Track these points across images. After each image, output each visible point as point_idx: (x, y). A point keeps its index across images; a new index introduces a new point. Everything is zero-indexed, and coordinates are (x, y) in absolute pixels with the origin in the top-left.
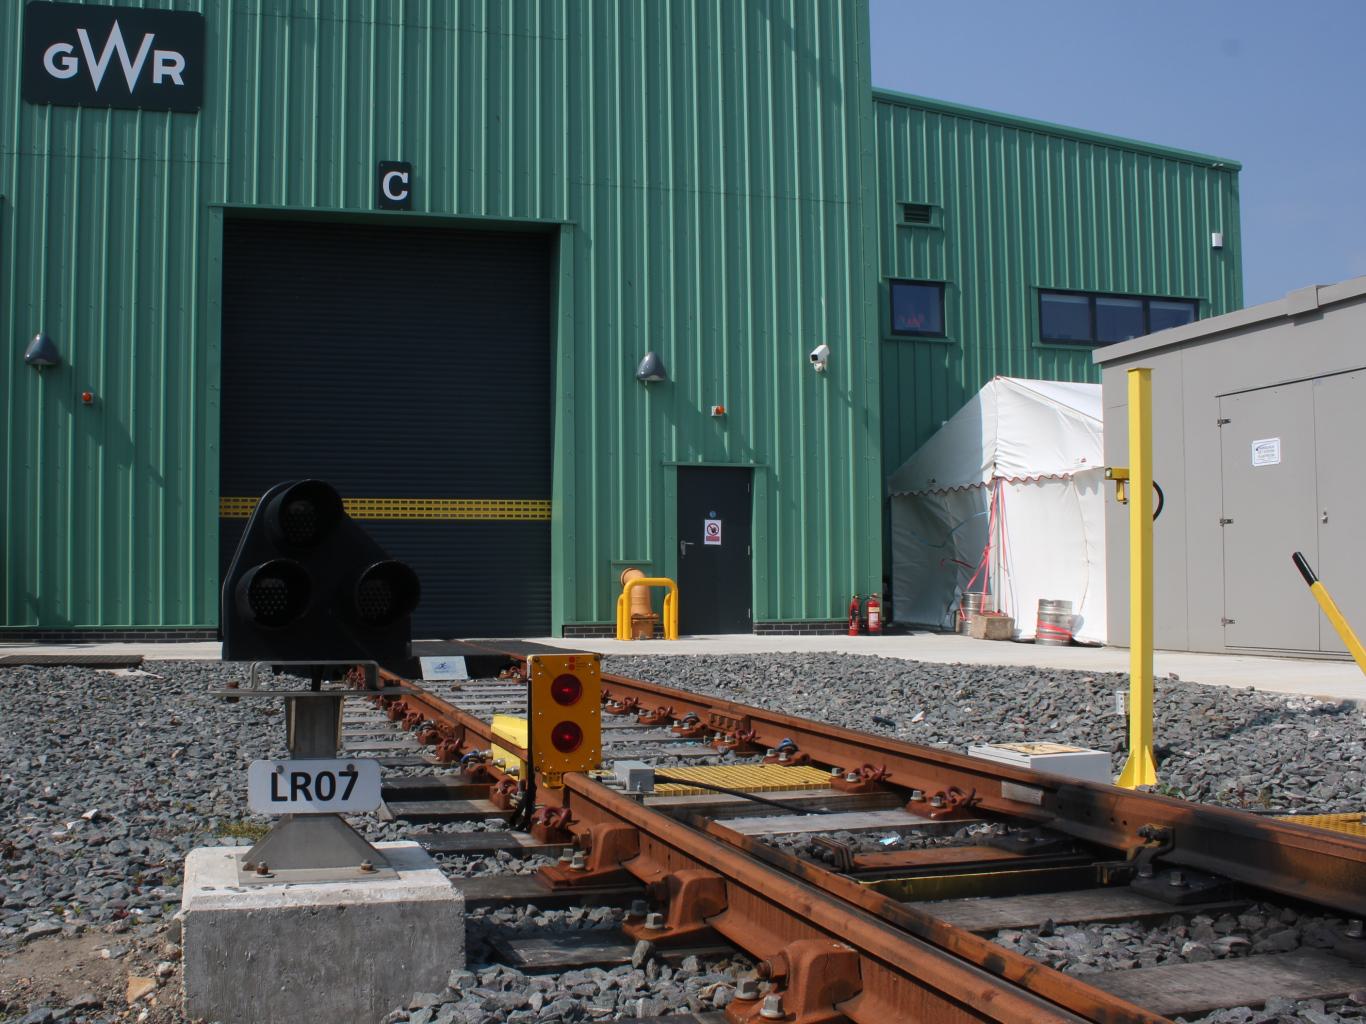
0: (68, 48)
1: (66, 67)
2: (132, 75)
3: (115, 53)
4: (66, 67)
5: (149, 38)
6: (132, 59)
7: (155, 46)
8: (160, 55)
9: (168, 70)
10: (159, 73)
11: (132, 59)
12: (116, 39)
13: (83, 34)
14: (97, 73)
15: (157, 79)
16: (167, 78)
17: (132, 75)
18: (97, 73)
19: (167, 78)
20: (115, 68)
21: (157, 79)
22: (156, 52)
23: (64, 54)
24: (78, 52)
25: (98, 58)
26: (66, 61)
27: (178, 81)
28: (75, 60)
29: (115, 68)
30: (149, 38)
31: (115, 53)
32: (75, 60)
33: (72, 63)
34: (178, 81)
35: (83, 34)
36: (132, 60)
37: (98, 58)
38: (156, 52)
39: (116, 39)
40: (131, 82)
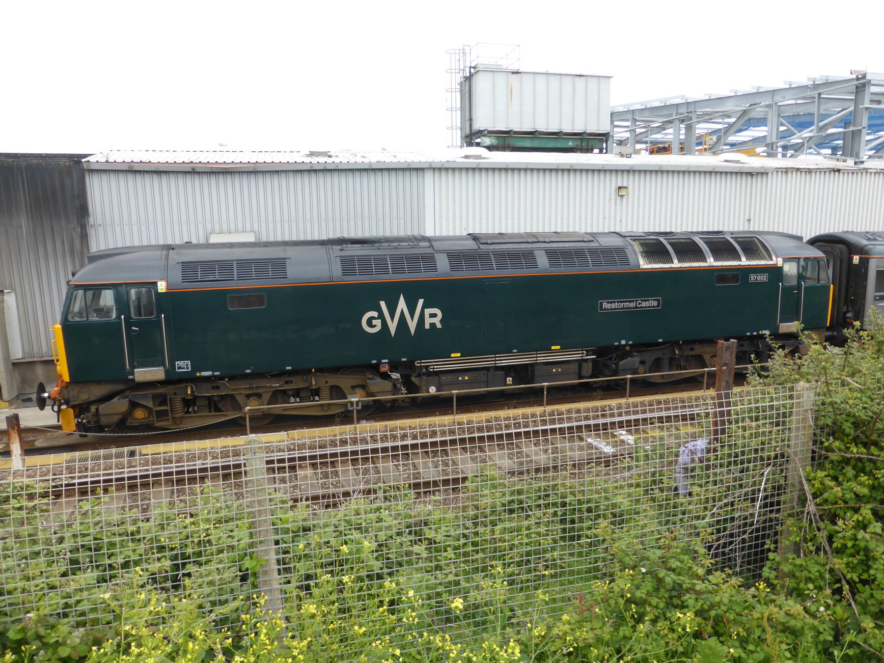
0: (375, 314)
1: (375, 326)
2: (412, 325)
4: (375, 326)
5: (421, 302)
6: (412, 316)
7: (425, 306)
8: (428, 311)
9: (433, 320)
10: (428, 321)
11: (412, 316)
12: (402, 305)
13: (383, 304)
14: (393, 327)
15: (427, 326)
16: (433, 325)
17: (412, 325)
18: (393, 327)
19: (433, 325)
21: (427, 326)
23: (372, 318)
24: (381, 316)
26: (374, 322)
27: (439, 326)
30: (421, 302)
33: (378, 323)
34: (439, 326)
35: (383, 304)
36: (412, 318)
37: (392, 319)
39: (402, 305)
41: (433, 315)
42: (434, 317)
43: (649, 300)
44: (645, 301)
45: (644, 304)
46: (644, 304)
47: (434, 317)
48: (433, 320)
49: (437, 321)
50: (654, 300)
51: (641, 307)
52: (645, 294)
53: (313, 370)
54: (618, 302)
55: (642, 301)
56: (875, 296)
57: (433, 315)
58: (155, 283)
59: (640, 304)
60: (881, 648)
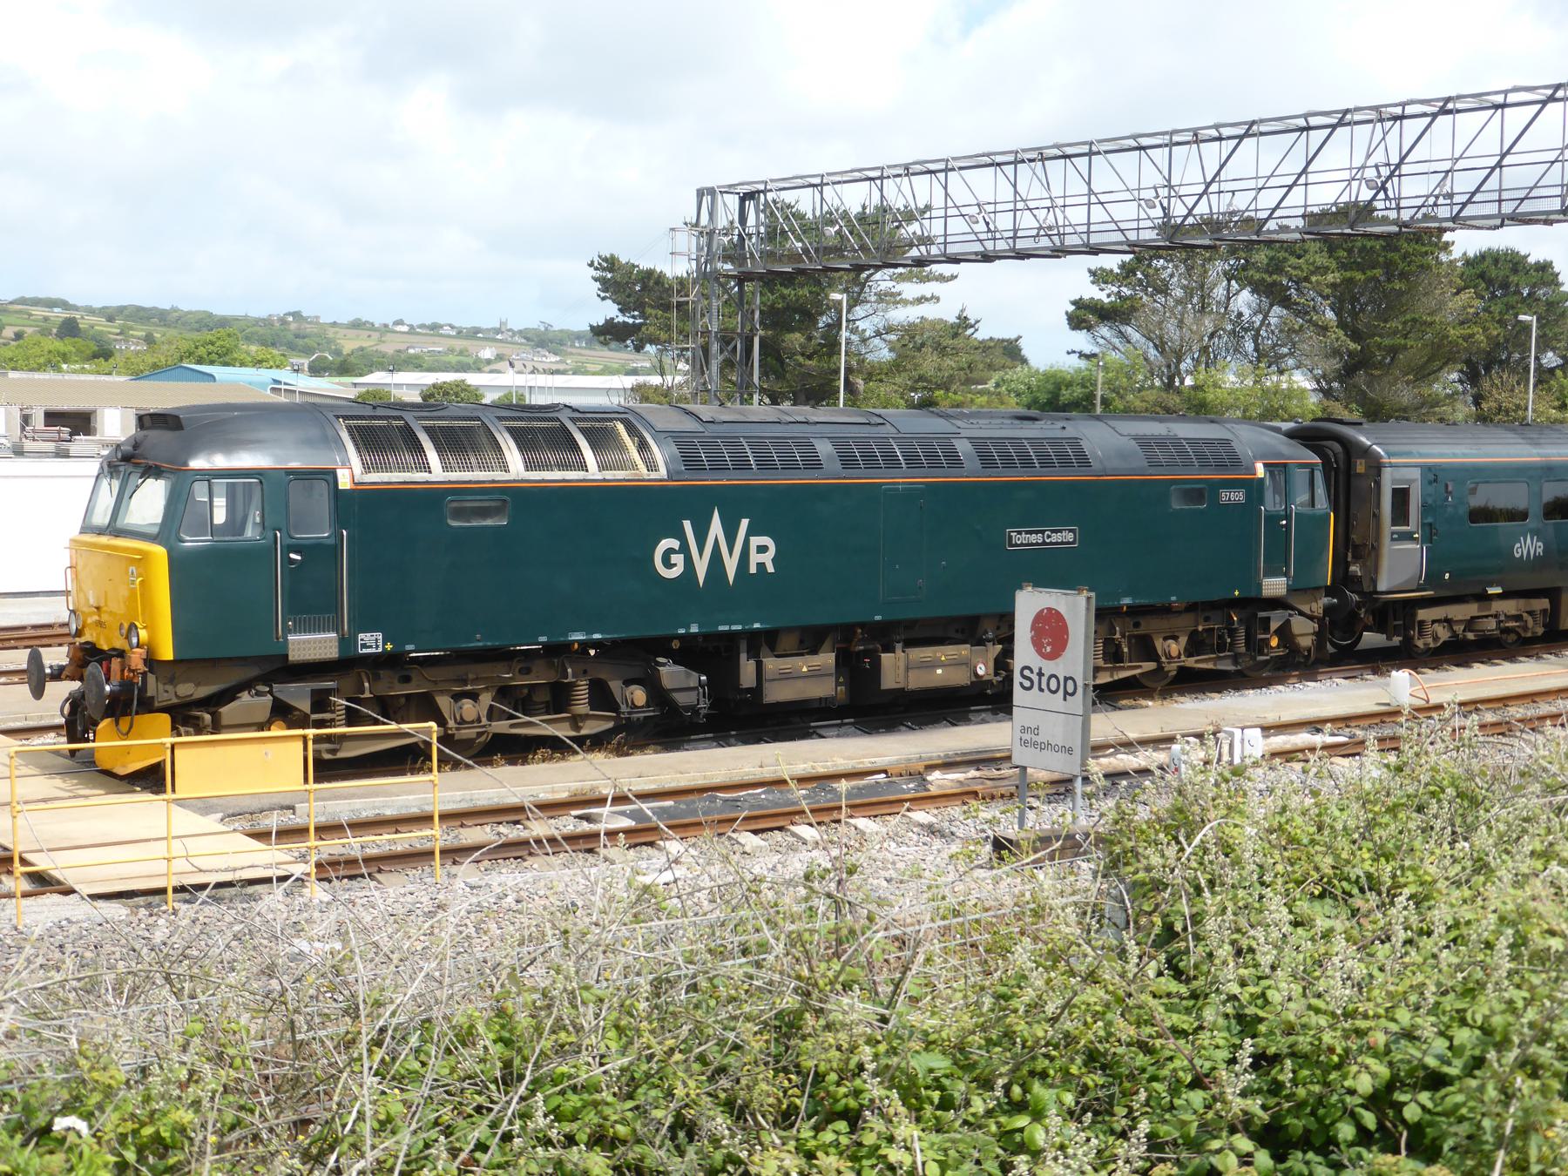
1: (675, 565)
2: (731, 565)
4: (675, 565)
5: (745, 523)
7: (750, 532)
8: (755, 541)
9: (762, 558)
10: (755, 558)
12: (716, 528)
13: (687, 525)
15: (753, 570)
16: (761, 566)
17: (731, 565)
19: (761, 566)
20: (716, 560)
21: (753, 570)
22: (752, 539)
23: (668, 553)
24: (684, 548)
27: (771, 569)
28: (682, 556)
29: (716, 560)
30: (745, 523)
32: (682, 556)
33: (678, 559)
34: (771, 569)
35: (687, 525)
38: (752, 539)
39: (716, 528)
41: (762, 549)
42: (764, 553)
43: (1060, 531)
44: (1056, 532)
45: (1056, 538)
46: (1056, 538)
47: (764, 553)
48: (762, 558)
49: (767, 558)
50: (1070, 531)
51: (1051, 543)
52: (1057, 523)
53: (576, 646)
54: (1027, 532)
55: (1053, 531)
56: (1393, 533)
57: (762, 549)
58: (333, 473)
59: (1049, 537)
60: (1425, 1148)
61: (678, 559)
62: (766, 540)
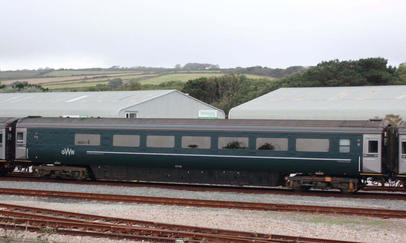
2: (69, 153)
3: (68, 152)
5: (71, 149)
7: (71, 150)
8: (72, 151)
12: (68, 150)
13: (65, 149)
14: (66, 153)
15: (72, 154)
16: (72, 154)
19: (72, 154)
20: (68, 153)
21: (72, 154)
23: (63, 152)
24: (65, 151)
25: (66, 151)
27: (74, 154)
29: (68, 153)
30: (71, 149)
31: (68, 152)
33: (64, 152)
35: (65, 149)
39: (68, 150)
40: (69, 154)
41: (73, 152)
47: (73, 152)
57: (73, 152)
61: (64, 152)
62: (73, 151)
